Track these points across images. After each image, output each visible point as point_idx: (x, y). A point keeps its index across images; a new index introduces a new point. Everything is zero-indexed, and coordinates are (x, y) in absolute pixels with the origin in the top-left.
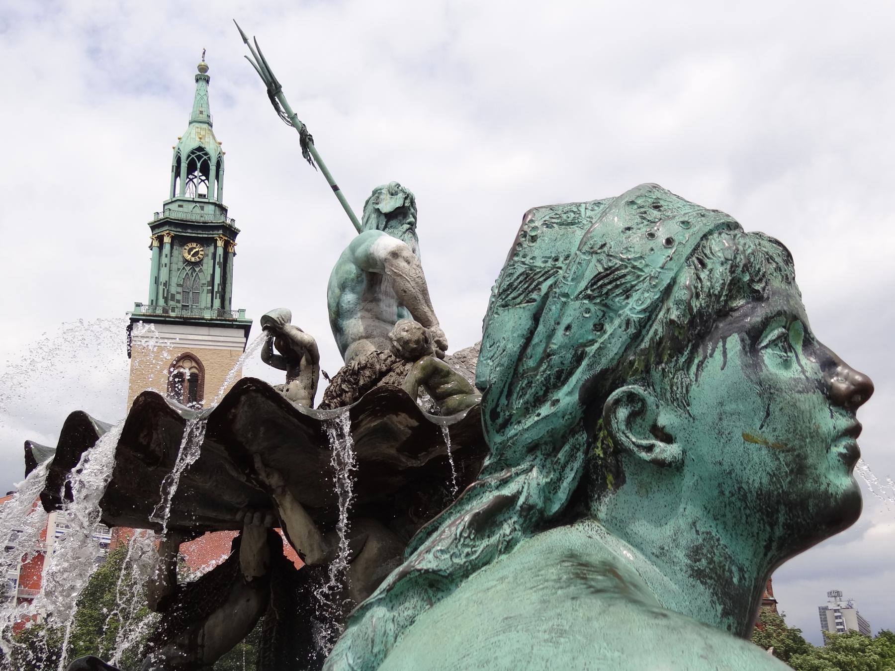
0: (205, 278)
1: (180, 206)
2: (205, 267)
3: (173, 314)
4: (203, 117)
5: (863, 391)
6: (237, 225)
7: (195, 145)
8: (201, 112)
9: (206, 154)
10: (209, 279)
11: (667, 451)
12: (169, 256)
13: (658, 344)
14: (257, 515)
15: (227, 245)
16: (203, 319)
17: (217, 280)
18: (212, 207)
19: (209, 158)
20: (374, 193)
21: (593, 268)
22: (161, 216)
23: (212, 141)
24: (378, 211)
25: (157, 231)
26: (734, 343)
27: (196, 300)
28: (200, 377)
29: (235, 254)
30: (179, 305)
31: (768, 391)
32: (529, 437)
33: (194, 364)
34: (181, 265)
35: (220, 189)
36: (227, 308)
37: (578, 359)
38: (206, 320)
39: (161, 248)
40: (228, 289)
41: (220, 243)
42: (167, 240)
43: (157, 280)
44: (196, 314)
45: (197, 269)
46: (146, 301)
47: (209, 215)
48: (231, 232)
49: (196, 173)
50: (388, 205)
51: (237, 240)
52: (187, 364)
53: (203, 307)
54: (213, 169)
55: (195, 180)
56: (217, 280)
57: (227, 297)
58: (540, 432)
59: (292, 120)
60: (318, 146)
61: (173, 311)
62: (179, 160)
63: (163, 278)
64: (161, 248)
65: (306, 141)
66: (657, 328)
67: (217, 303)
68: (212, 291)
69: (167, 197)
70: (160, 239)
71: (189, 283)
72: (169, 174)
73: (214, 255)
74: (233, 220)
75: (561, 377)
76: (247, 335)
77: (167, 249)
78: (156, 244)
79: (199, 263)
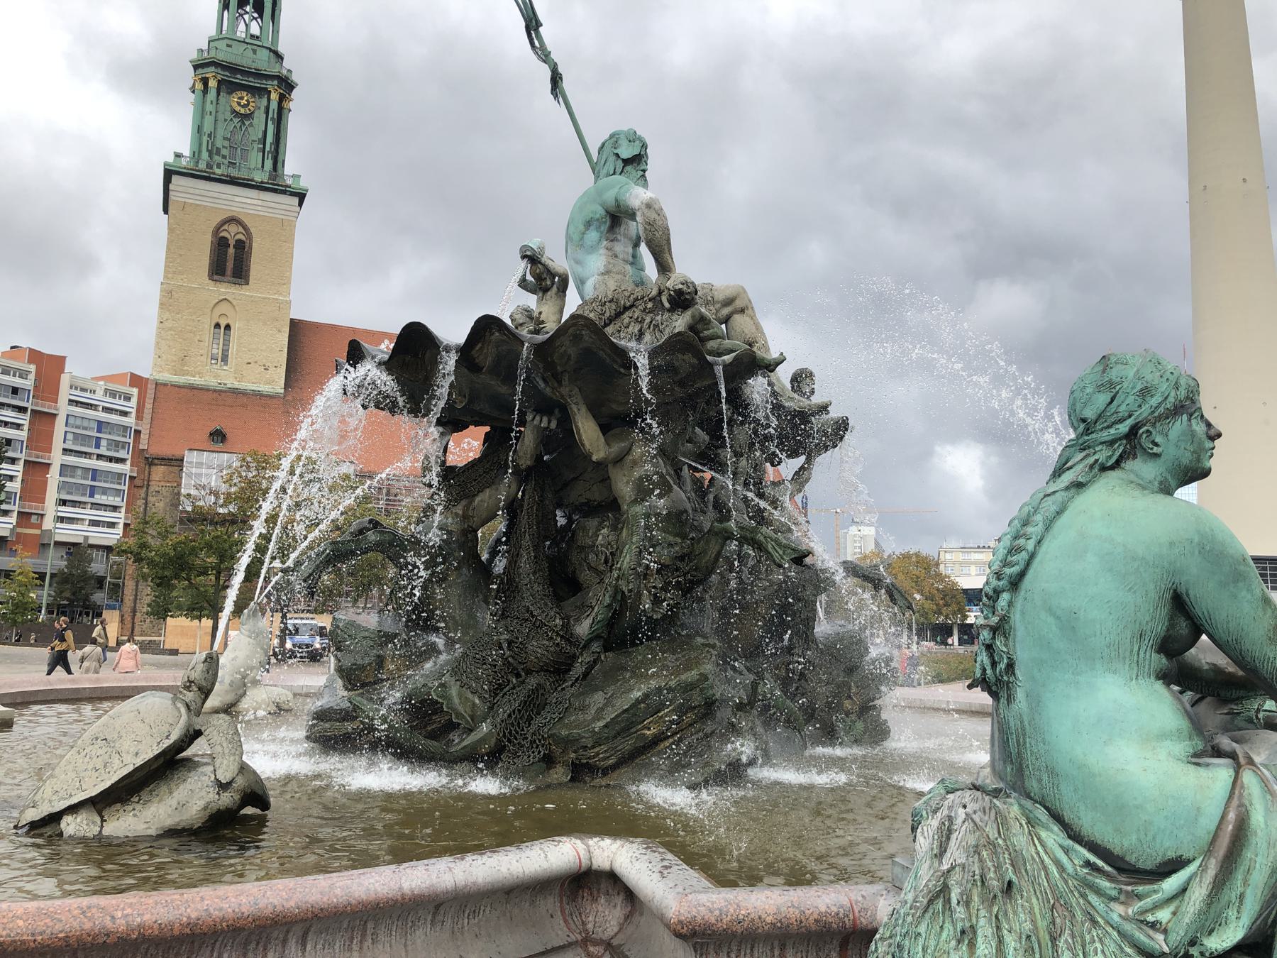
1: (228, 46)
2: (255, 121)
3: (218, 171)
5: (1219, 435)
6: (294, 78)
10: (260, 136)
11: (1156, 450)
13: (1160, 415)
14: (538, 418)
15: (282, 98)
17: (270, 138)
18: (266, 52)
20: (612, 136)
21: (1139, 387)
22: (206, 55)
24: (617, 155)
26: (1185, 417)
27: (245, 157)
28: (247, 245)
30: (226, 162)
31: (1193, 434)
32: (1103, 440)
33: (241, 230)
34: (228, 116)
35: (276, 32)
36: (279, 171)
37: (1130, 416)
41: (274, 96)
42: (213, 84)
43: (199, 129)
45: (247, 123)
46: (187, 152)
47: (262, 61)
48: (287, 85)
49: (248, 8)
50: (627, 152)
51: (294, 94)
52: (233, 229)
55: (246, 17)
56: (270, 138)
58: (1110, 438)
59: (545, 56)
60: (566, 84)
61: (219, 166)
63: (208, 127)
65: (556, 79)
66: (1162, 409)
67: (269, 164)
69: (213, 32)
70: (205, 81)
71: (238, 137)
73: (267, 109)
74: (289, 71)
75: (1121, 421)
76: (300, 205)
77: (212, 94)
78: (199, 86)
79: (249, 116)
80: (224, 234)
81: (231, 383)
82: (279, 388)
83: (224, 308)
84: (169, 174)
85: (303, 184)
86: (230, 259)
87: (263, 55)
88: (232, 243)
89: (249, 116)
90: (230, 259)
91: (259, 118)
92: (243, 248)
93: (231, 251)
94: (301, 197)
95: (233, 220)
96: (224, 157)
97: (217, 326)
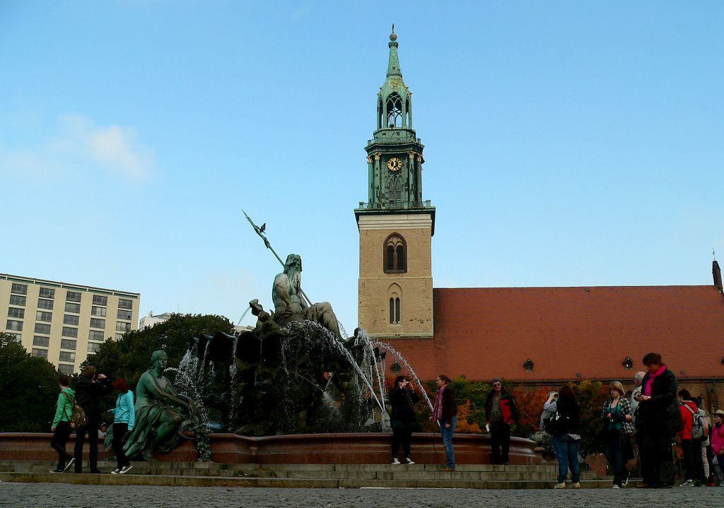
0: (403, 181)
1: (385, 134)
3: (383, 208)
4: (396, 71)
6: (422, 143)
7: (391, 92)
8: (394, 68)
9: (399, 96)
12: (379, 168)
15: (416, 156)
16: (403, 209)
17: (411, 182)
18: (404, 132)
19: (401, 99)
22: (373, 142)
23: (402, 87)
25: (370, 153)
29: (423, 161)
33: (400, 240)
34: (387, 174)
35: (410, 119)
36: (419, 200)
38: (405, 210)
39: (373, 164)
40: (419, 187)
41: (412, 157)
42: (377, 158)
43: (372, 186)
44: (398, 206)
45: (398, 176)
46: (366, 201)
48: (419, 148)
52: (395, 240)
53: (403, 200)
54: (404, 106)
56: (411, 182)
57: (419, 192)
62: (381, 103)
64: (373, 164)
67: (412, 197)
68: (408, 190)
69: (376, 129)
70: (373, 158)
72: (375, 113)
73: (408, 164)
76: (433, 218)
77: (377, 164)
79: (399, 171)
80: (391, 244)
81: (403, 334)
82: (431, 334)
83: (395, 288)
84: (358, 215)
85: (432, 205)
86: (395, 257)
87: (403, 134)
88: (395, 248)
89: (399, 171)
90: (395, 257)
91: (404, 173)
92: (402, 251)
93: (395, 254)
94: (432, 213)
95: (395, 235)
96: (387, 198)
97: (392, 299)
